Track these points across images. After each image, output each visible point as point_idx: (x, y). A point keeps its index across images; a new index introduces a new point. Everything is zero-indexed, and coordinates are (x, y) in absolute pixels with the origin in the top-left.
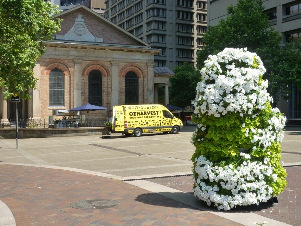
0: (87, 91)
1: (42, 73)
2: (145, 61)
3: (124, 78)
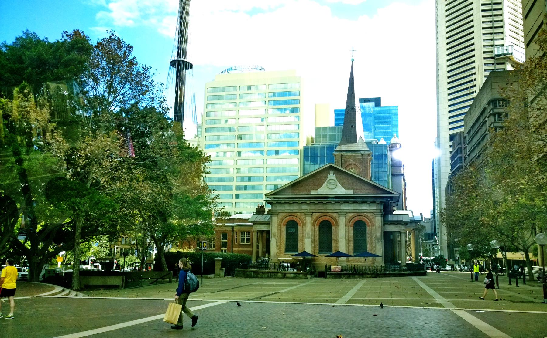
0: (317, 239)
1: (280, 224)
2: (371, 211)
3: (352, 227)
